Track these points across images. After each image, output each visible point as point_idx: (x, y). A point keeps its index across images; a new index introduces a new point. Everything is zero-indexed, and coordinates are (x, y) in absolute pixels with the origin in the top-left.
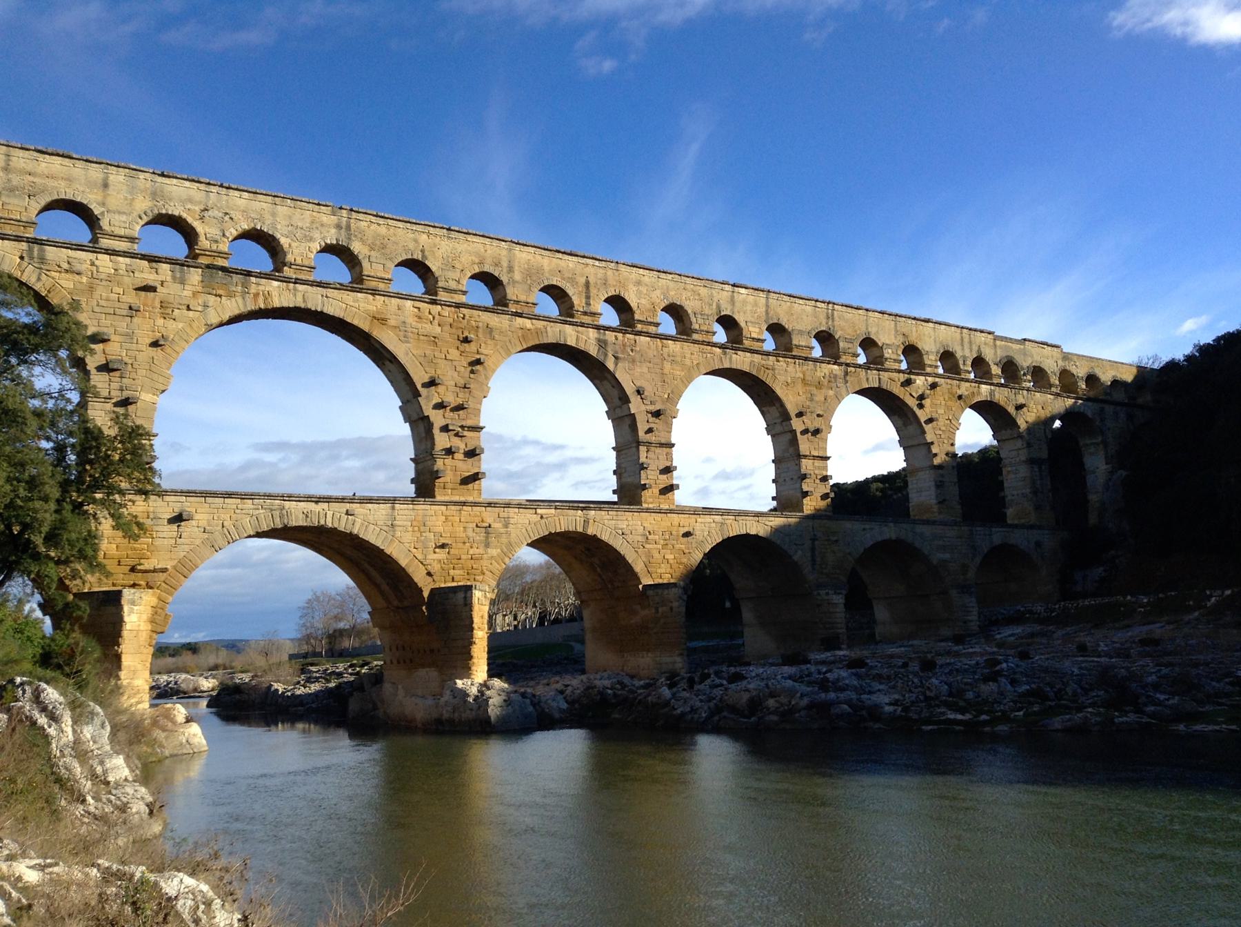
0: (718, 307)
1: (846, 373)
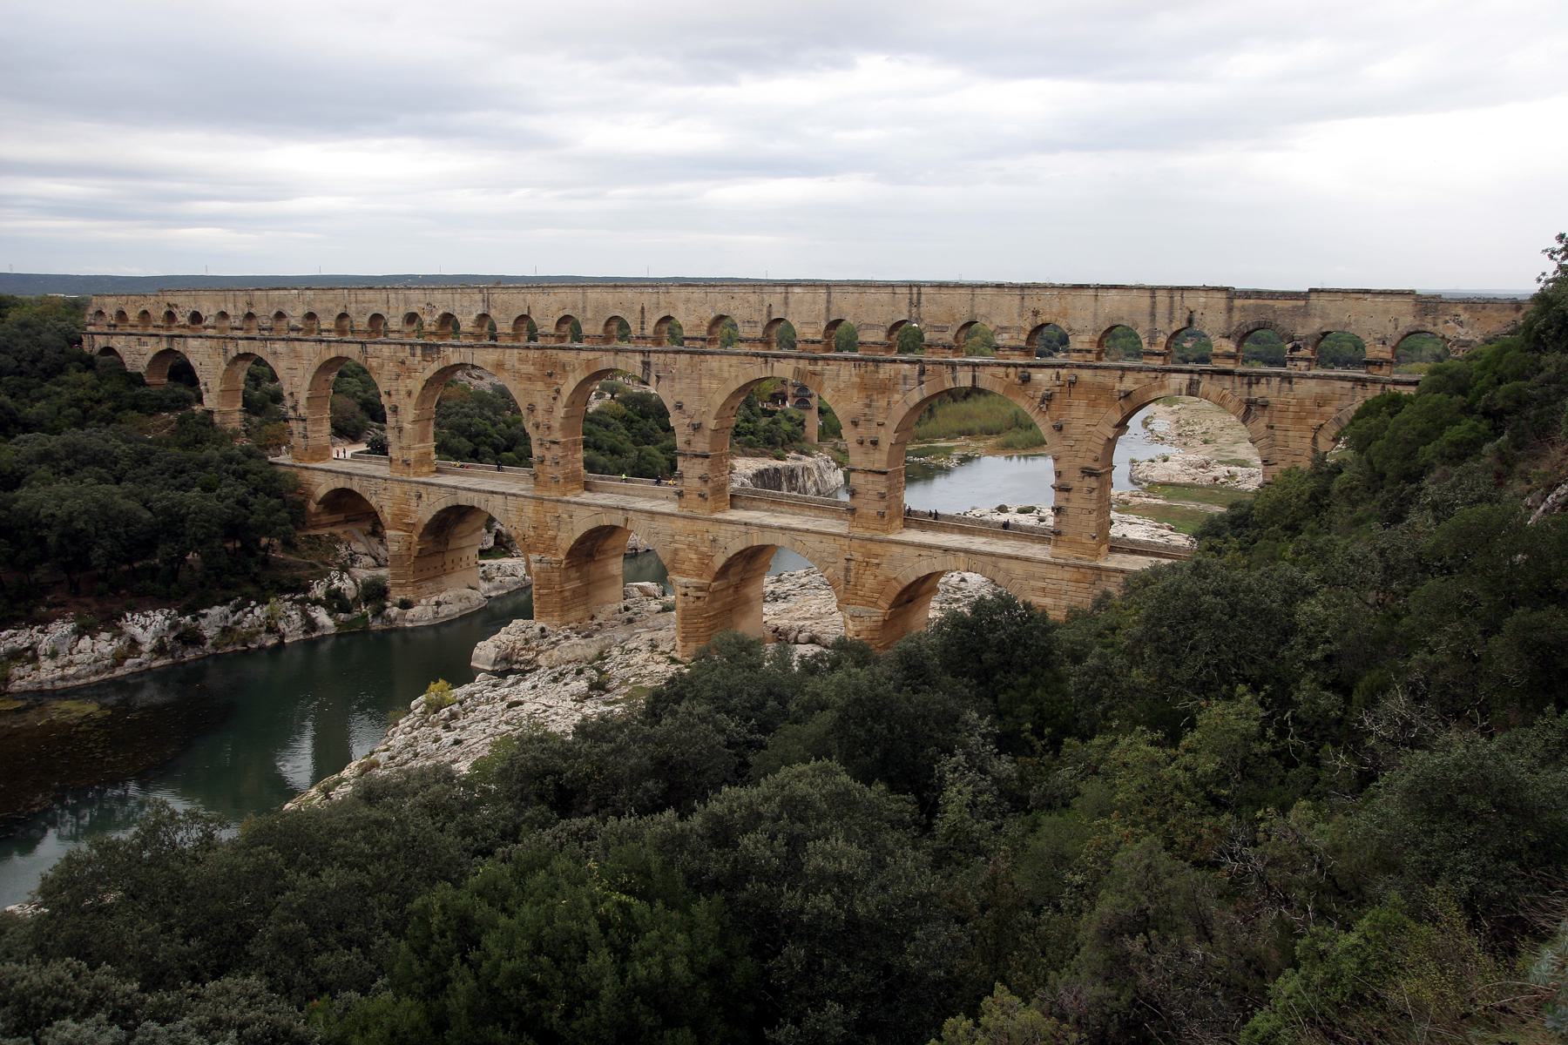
0: (769, 313)
1: (922, 372)
